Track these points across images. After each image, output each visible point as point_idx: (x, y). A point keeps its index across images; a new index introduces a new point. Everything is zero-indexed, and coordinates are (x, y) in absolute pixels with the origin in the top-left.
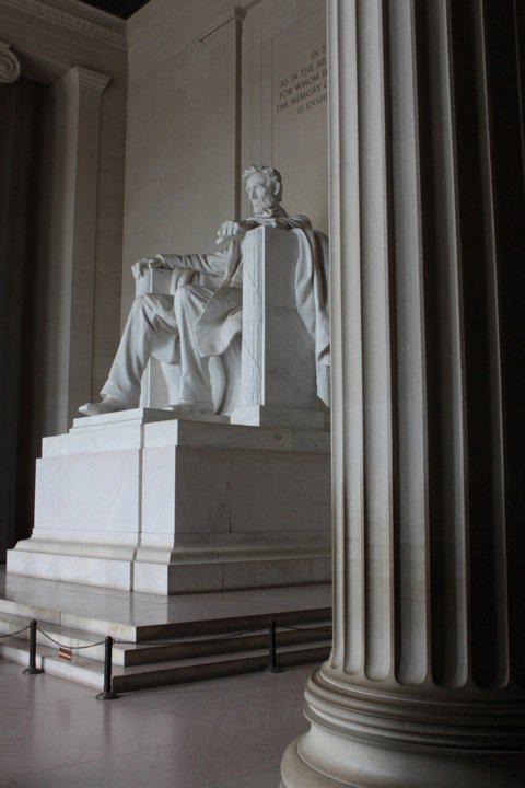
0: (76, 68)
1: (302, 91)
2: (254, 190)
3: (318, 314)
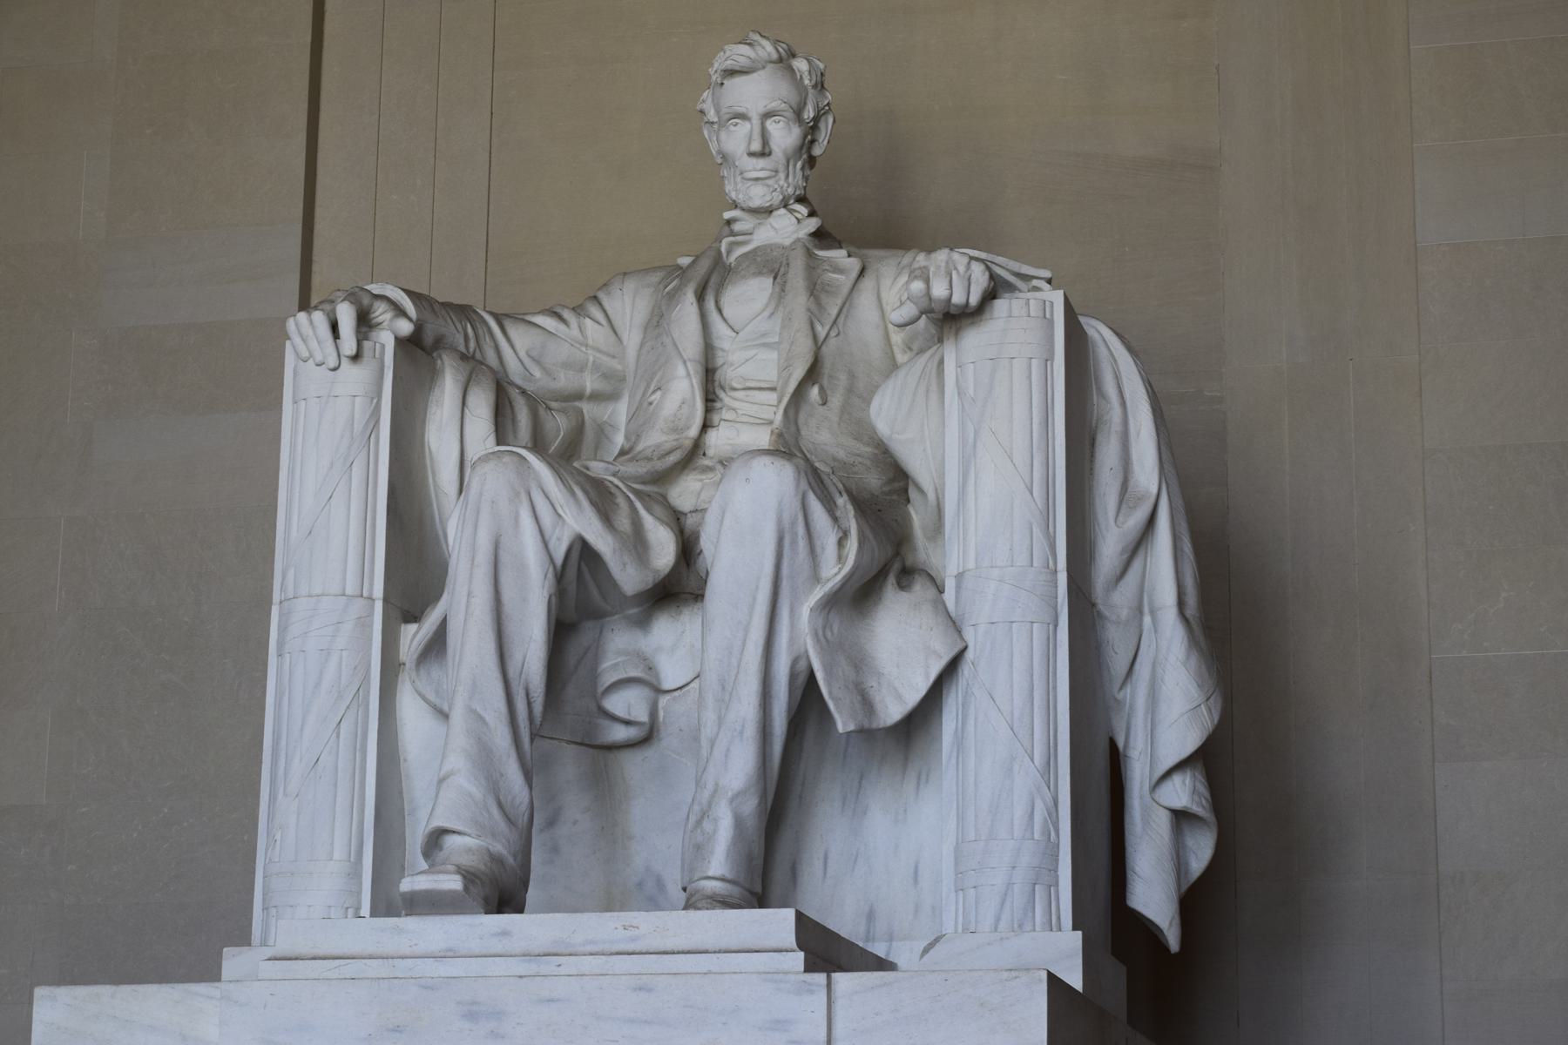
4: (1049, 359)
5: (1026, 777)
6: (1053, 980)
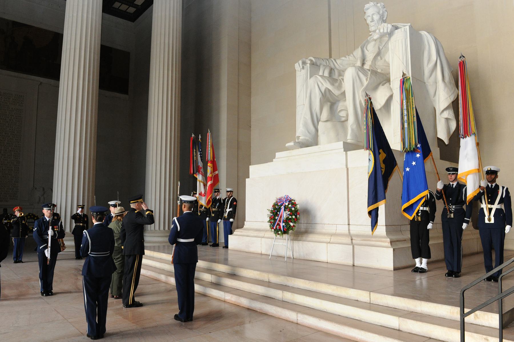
2: (372, 17)
3: (441, 85)
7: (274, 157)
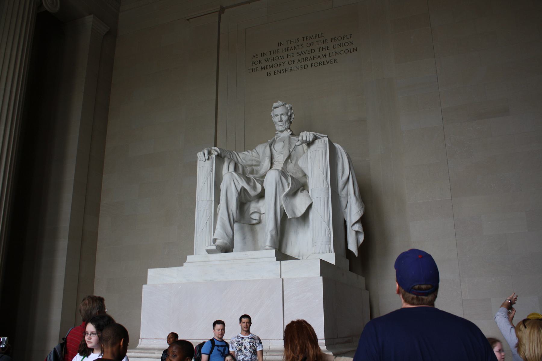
0: (92, 16)
1: (270, 63)
4: (326, 150)
5: (324, 225)
6: (321, 260)
7: (185, 261)
